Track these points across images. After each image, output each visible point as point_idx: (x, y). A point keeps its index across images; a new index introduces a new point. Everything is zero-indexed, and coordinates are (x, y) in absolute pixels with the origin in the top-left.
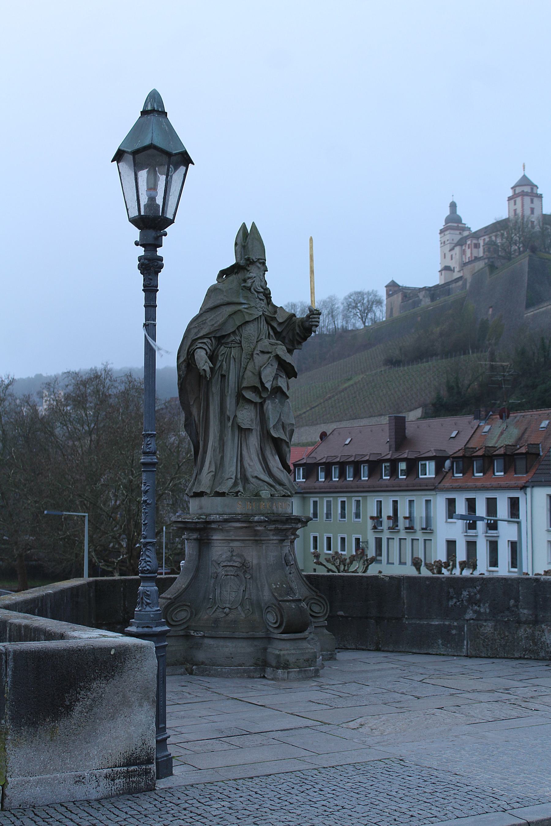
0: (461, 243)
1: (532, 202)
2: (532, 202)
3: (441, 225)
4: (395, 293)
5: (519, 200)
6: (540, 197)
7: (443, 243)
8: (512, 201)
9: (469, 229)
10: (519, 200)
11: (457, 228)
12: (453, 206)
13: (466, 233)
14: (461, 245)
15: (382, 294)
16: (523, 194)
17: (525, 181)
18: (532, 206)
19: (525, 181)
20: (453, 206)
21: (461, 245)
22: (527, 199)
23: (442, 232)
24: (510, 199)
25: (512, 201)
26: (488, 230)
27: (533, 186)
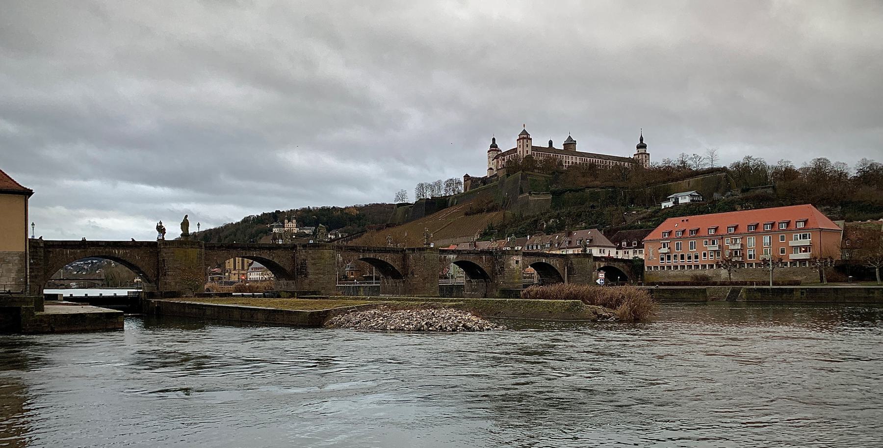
0: (496, 157)
1: (527, 142)
2: (527, 142)
3: (489, 149)
4: (468, 180)
5: (522, 140)
6: (531, 139)
7: (489, 157)
8: (519, 141)
9: (501, 151)
10: (522, 140)
11: (495, 150)
12: (494, 139)
13: (499, 153)
14: (497, 159)
15: (462, 180)
16: (523, 138)
17: (524, 132)
18: (527, 144)
19: (524, 132)
20: (494, 139)
21: (497, 159)
22: (525, 140)
23: (488, 152)
24: (518, 140)
25: (519, 141)
26: (508, 152)
27: (527, 134)
